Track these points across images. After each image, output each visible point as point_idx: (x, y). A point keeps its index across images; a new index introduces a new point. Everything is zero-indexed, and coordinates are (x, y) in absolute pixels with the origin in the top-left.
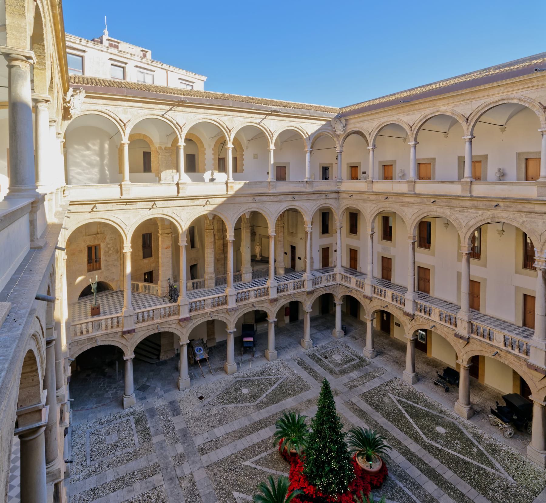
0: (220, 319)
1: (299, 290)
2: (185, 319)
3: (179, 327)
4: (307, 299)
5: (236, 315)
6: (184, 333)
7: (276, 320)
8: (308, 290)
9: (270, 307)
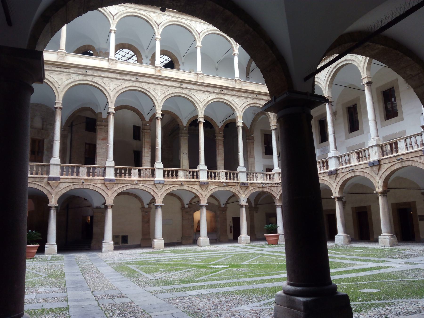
0: (146, 190)
2: (110, 180)
3: (104, 188)
4: (241, 192)
5: (164, 189)
8: (241, 181)
9: (200, 190)
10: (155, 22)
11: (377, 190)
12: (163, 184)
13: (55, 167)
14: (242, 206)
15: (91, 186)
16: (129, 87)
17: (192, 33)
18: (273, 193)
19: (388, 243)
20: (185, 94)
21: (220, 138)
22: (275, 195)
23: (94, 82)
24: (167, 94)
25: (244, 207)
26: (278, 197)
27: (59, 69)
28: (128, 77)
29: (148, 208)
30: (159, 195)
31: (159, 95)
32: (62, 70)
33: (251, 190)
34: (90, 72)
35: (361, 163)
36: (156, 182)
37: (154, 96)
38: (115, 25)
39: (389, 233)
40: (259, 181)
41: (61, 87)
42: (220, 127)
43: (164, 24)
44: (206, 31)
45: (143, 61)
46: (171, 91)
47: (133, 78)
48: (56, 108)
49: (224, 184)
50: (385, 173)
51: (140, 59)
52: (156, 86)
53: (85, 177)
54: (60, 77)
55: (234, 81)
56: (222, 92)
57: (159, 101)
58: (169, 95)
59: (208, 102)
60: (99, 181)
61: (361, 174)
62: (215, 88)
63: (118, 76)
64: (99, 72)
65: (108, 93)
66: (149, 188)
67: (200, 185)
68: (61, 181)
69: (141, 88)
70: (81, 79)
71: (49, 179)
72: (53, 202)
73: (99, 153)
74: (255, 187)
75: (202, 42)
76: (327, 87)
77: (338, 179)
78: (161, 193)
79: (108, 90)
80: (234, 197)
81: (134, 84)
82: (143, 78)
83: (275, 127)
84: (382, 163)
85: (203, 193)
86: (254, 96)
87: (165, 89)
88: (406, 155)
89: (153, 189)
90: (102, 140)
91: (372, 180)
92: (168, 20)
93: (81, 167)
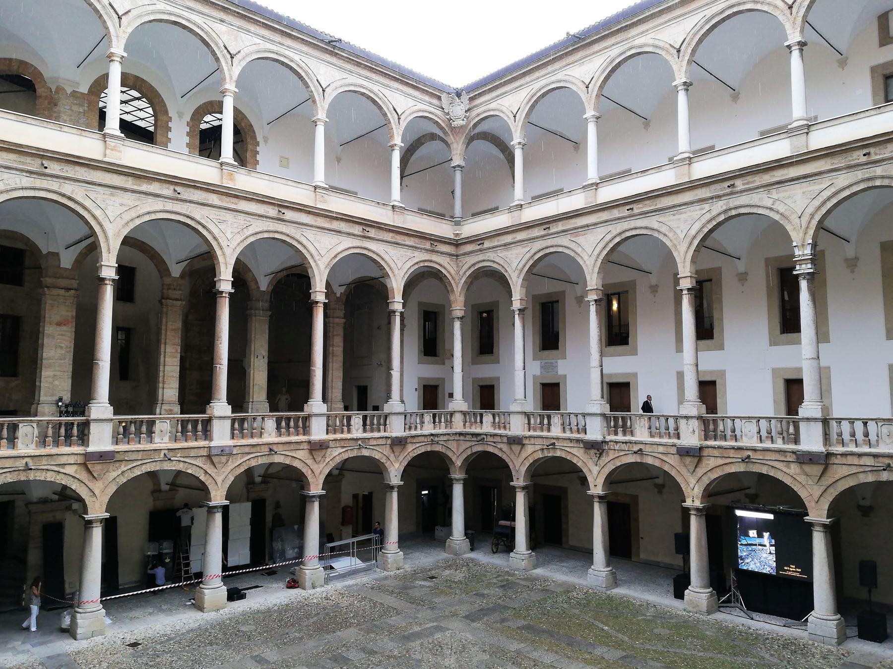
0: (189, 471)
1: (376, 434)
2: (103, 457)
3: (83, 475)
5: (231, 465)
7: (324, 492)
8: (394, 435)
10: (226, 48)
11: (688, 503)
14: (392, 488)
15: (49, 474)
17: (307, 87)
18: (450, 454)
19: (705, 609)
21: (337, 320)
22: (454, 459)
23: (64, 195)
25: (396, 489)
26: (459, 463)
28: (155, 188)
29: (170, 490)
30: (219, 480)
31: (229, 236)
33: (412, 450)
34: (54, 168)
35: (657, 440)
37: (215, 238)
38: (124, 41)
39: (705, 587)
40: (426, 432)
42: (338, 295)
43: (247, 55)
44: (338, 84)
45: (170, 124)
46: (259, 226)
47: (167, 191)
49: (360, 442)
50: (709, 474)
51: (165, 118)
52: (223, 213)
53: (32, 450)
55: (390, 208)
56: (367, 234)
59: (336, 256)
60: (72, 460)
61: (657, 463)
62: (351, 224)
63: (129, 183)
64: (77, 168)
65: (101, 226)
66: (196, 468)
67: (311, 451)
69: (184, 215)
70: (28, 185)
73: (48, 359)
74: (418, 445)
75: (328, 111)
76: (596, 270)
77: (605, 459)
78: (223, 477)
79: (100, 219)
80: (376, 469)
81: (170, 206)
82: (192, 190)
83: (460, 314)
84: (706, 452)
86: (428, 245)
87: (242, 222)
88: (759, 453)
89: (205, 467)
90: (59, 324)
91: (679, 479)
92: (255, 48)
93: (21, 425)
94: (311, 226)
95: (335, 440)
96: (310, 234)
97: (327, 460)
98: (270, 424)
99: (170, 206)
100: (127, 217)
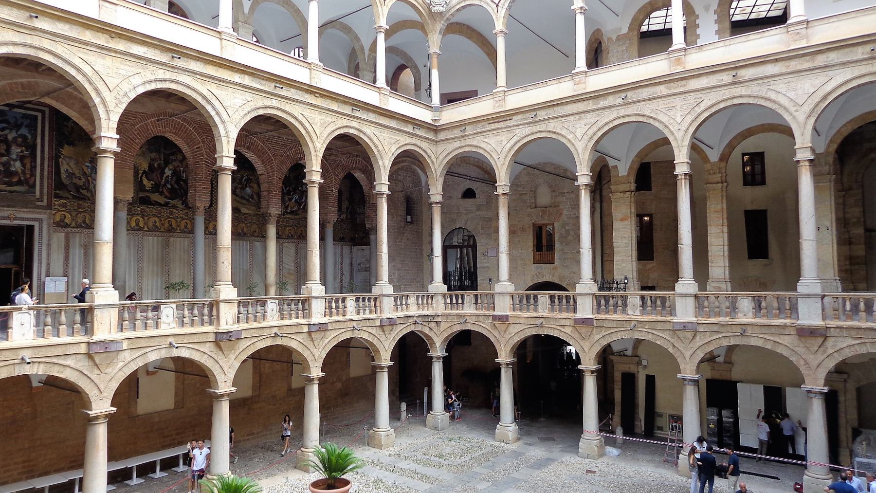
0: (658, 342)
2: (585, 322)
3: (576, 336)
5: (699, 341)
6: (586, 349)
9: (801, 350)
12: (695, 333)
13: (501, 297)
15: (556, 331)
16: (611, 121)
20: (749, 96)
23: (549, 132)
24: (698, 110)
27: (497, 126)
30: (688, 354)
32: (501, 125)
34: (542, 115)
36: (678, 327)
41: (502, 156)
48: (498, 195)
51: (693, 18)
54: (499, 138)
57: (679, 135)
58: (703, 112)
59: (825, 98)
68: (511, 321)
71: (495, 318)
72: (504, 357)
81: (623, 111)
82: (640, 90)
85: (810, 358)
89: (672, 340)
90: (622, 220)
94: (781, 75)
95: (841, 328)
96: (780, 85)
97: (830, 351)
98: (745, 304)
99: (623, 111)
100: (590, 133)
